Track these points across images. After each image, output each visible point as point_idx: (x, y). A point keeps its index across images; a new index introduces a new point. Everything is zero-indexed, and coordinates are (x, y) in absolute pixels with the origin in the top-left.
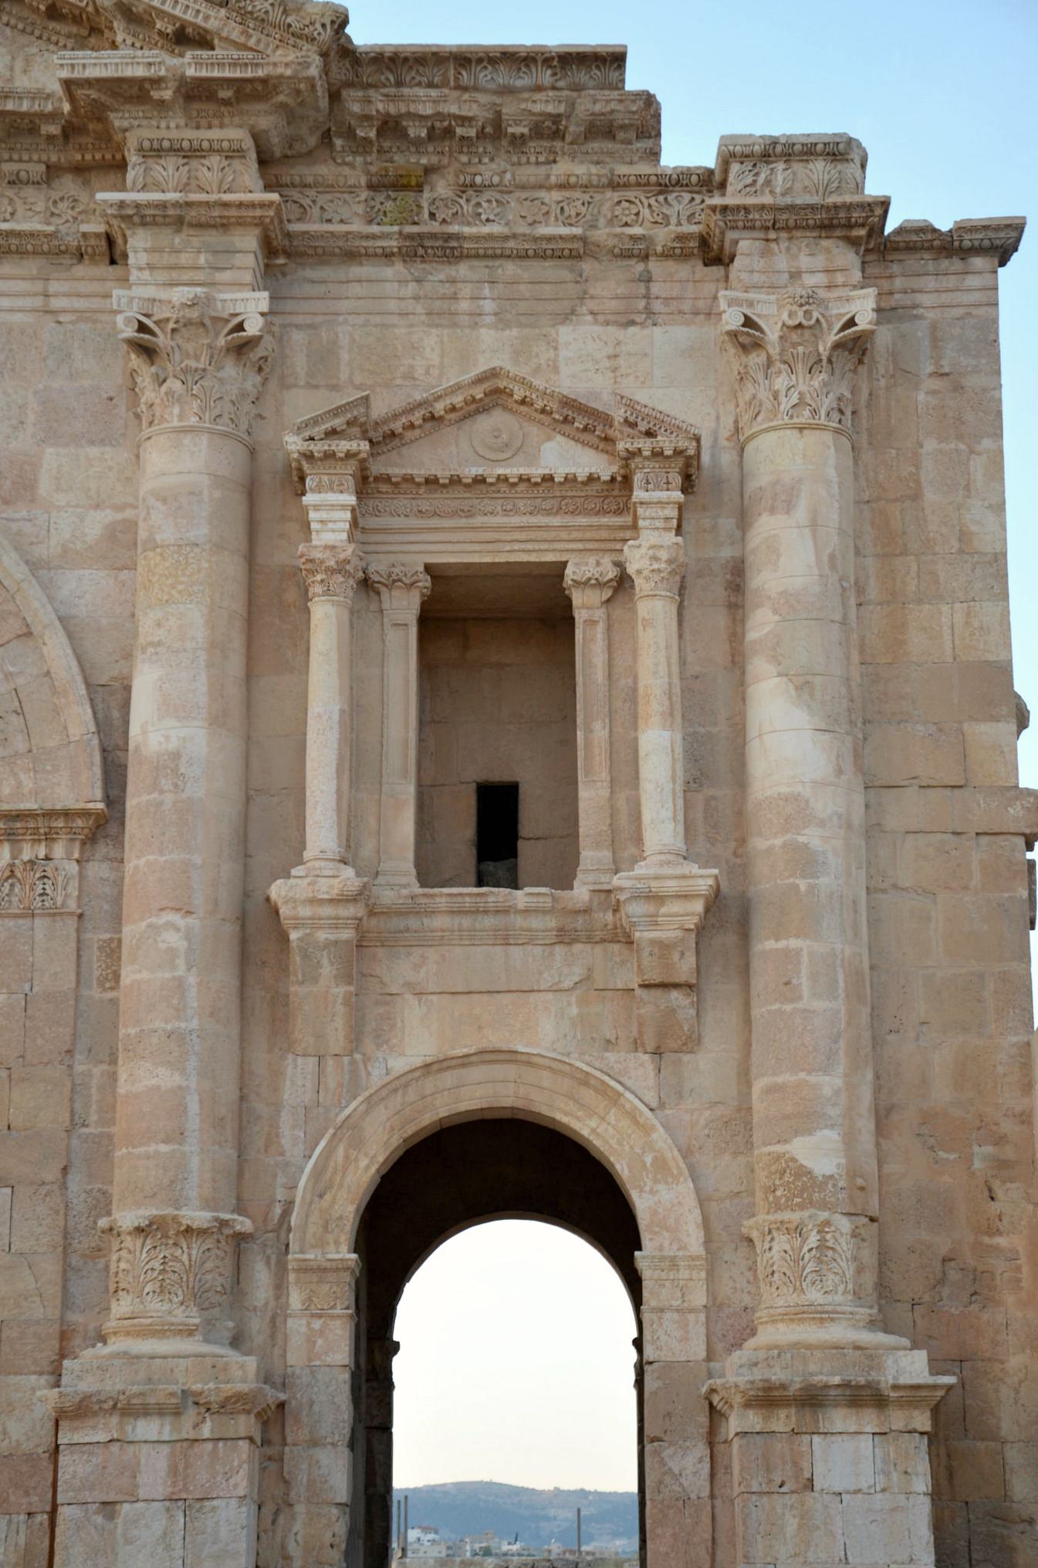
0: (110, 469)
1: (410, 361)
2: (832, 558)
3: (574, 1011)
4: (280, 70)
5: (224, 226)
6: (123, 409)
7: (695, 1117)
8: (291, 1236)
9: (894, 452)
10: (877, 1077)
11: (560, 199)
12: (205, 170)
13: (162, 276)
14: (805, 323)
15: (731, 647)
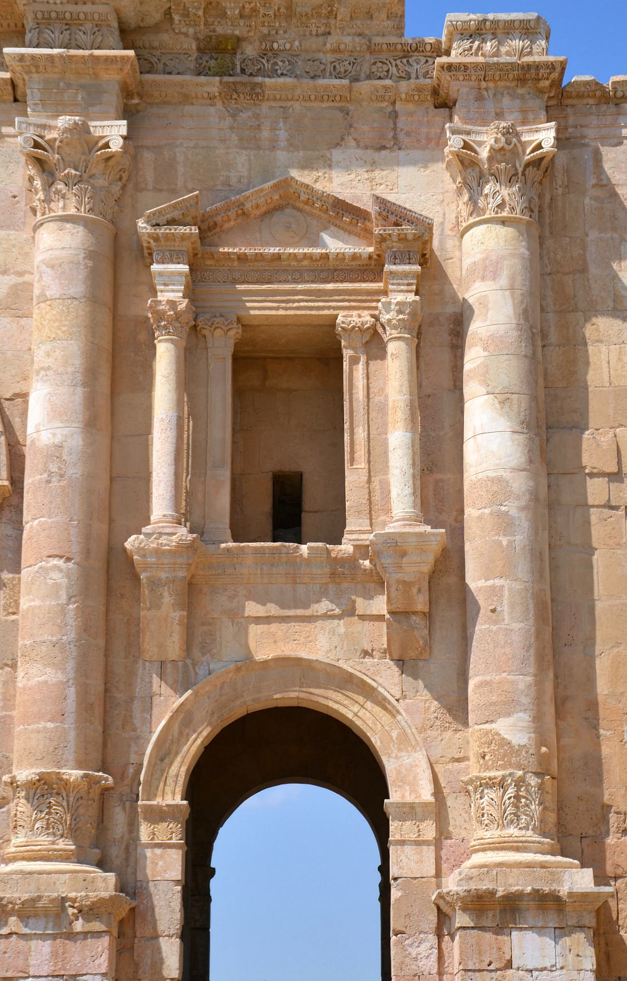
0: (14, 246)
1: (227, 173)
2: (525, 311)
3: (342, 630)
6: (23, 204)
7: (427, 705)
8: (140, 788)
9: (568, 239)
10: (556, 677)
11: (333, 60)
12: (81, 33)
14: (506, 146)
15: (453, 375)
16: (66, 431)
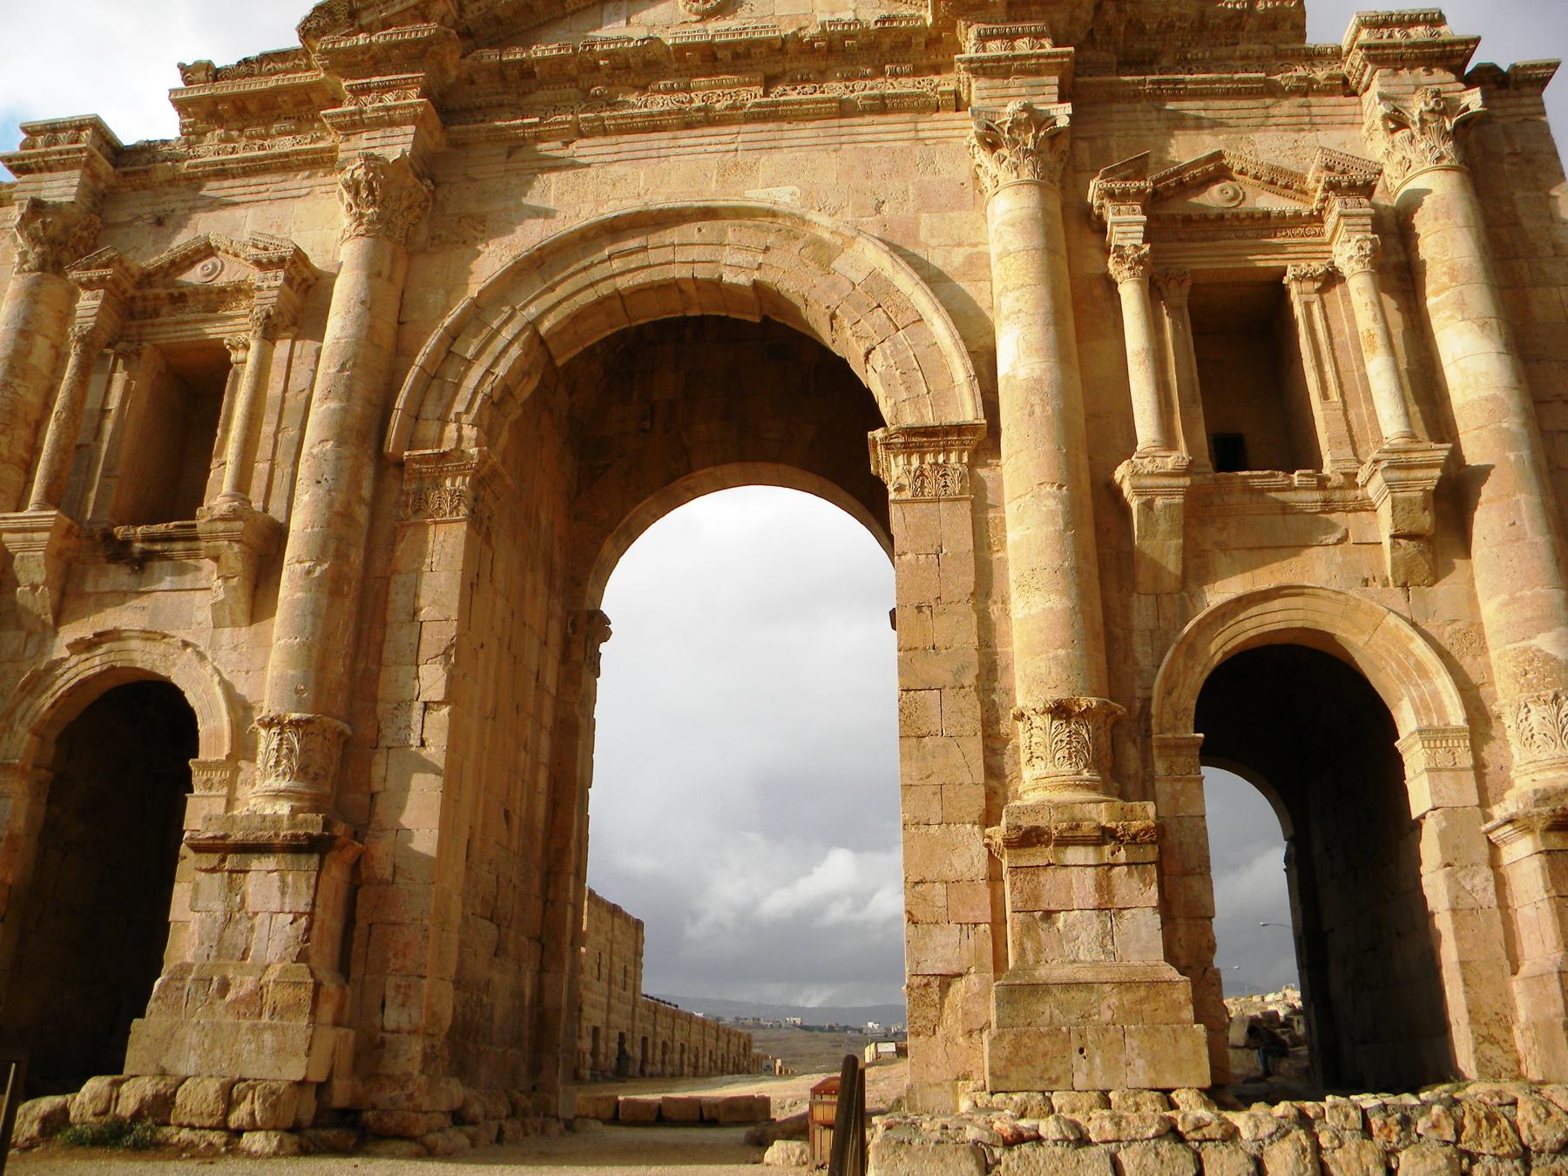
3: (1339, 559)
5: (1037, 72)
8: (1153, 721)
16: (1044, 366)
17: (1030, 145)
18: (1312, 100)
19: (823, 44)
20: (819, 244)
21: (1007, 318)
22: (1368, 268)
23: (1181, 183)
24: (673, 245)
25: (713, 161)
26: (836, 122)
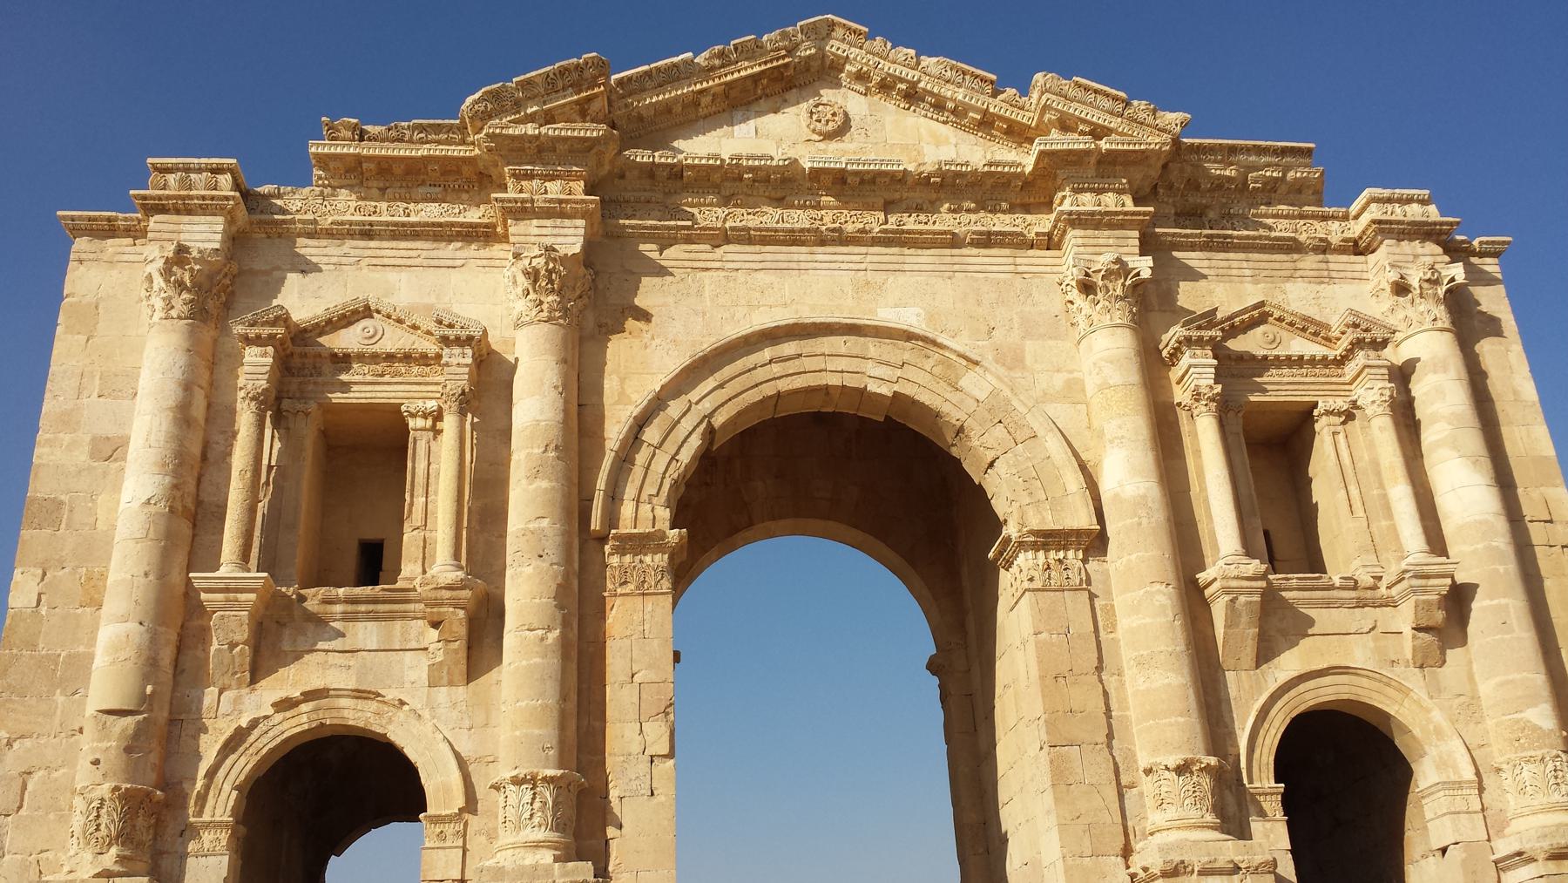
0: (1062, 351)
3: (1371, 644)
4: (1152, 146)
13: (1090, 250)
17: (1119, 292)
18: (1330, 257)
19: (938, 179)
20: (946, 362)
21: (1111, 442)
22: (1388, 411)
23: (1232, 326)
24: (823, 354)
25: (846, 277)
26: (948, 251)
